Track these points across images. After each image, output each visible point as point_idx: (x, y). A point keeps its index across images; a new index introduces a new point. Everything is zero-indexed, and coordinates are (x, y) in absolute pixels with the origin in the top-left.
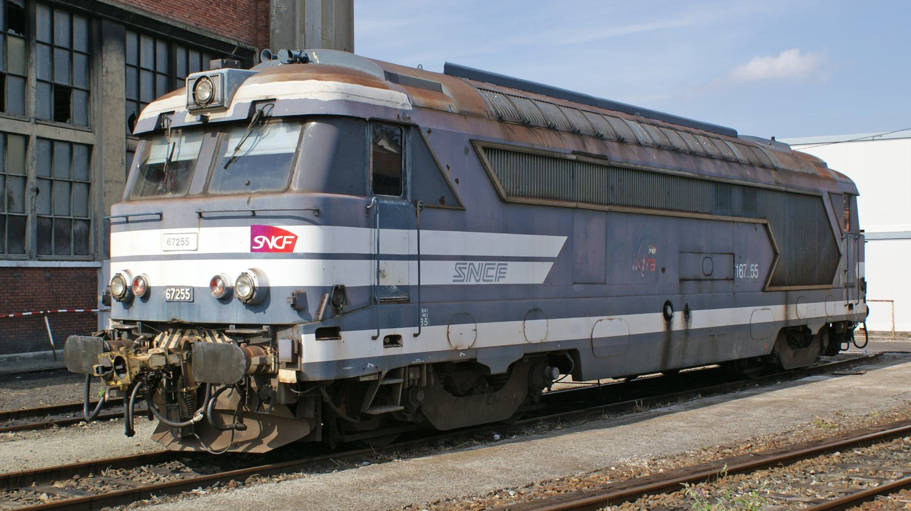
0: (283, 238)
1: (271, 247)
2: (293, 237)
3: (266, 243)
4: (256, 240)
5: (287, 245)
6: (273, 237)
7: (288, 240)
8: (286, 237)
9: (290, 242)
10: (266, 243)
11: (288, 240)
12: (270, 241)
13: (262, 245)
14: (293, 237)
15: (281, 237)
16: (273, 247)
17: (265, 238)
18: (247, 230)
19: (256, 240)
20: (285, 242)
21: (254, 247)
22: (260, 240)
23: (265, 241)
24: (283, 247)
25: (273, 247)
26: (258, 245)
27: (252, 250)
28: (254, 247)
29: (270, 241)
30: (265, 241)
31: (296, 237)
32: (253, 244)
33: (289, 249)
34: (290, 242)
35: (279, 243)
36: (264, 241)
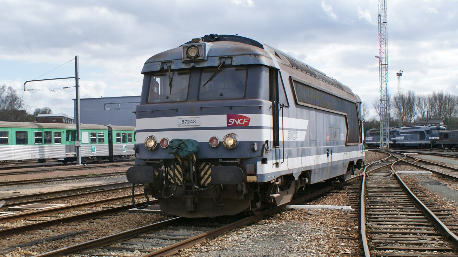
0: (243, 120)
1: (237, 124)
2: (248, 119)
3: (235, 122)
4: (230, 121)
5: (245, 122)
6: (238, 119)
7: (246, 120)
9: (247, 121)
10: (235, 122)
11: (246, 120)
13: (233, 123)
14: (248, 119)
15: (243, 119)
16: (239, 124)
17: (234, 120)
18: (225, 116)
19: (230, 121)
20: (244, 121)
21: (229, 124)
22: (232, 121)
23: (235, 121)
24: (244, 123)
25: (239, 124)
26: (231, 123)
27: (228, 125)
28: (229, 124)
30: (235, 121)
31: (250, 119)
32: (228, 122)
33: (247, 124)
34: (247, 121)
35: (242, 122)
36: (234, 121)
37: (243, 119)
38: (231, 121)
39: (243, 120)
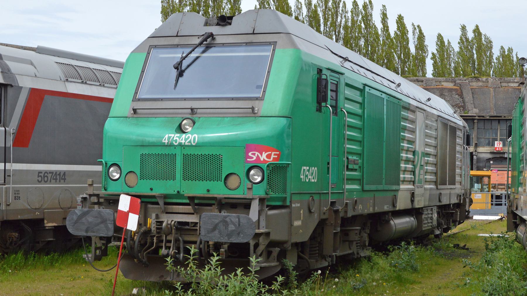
0: (272, 153)
1: (262, 159)
4: (250, 154)
5: (274, 158)
6: (264, 153)
8: (273, 153)
9: (276, 156)
12: (262, 155)
13: (255, 158)
15: (270, 153)
16: (264, 159)
17: (257, 153)
19: (250, 154)
20: (273, 156)
22: (254, 154)
23: (258, 155)
25: (264, 159)
26: (252, 158)
28: (248, 160)
29: (262, 155)
30: (258, 155)
34: (276, 156)
35: (269, 156)
36: (256, 155)
37: (270, 153)
38: (252, 154)
39: (270, 155)
